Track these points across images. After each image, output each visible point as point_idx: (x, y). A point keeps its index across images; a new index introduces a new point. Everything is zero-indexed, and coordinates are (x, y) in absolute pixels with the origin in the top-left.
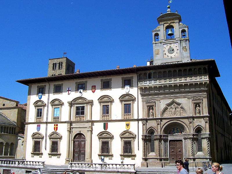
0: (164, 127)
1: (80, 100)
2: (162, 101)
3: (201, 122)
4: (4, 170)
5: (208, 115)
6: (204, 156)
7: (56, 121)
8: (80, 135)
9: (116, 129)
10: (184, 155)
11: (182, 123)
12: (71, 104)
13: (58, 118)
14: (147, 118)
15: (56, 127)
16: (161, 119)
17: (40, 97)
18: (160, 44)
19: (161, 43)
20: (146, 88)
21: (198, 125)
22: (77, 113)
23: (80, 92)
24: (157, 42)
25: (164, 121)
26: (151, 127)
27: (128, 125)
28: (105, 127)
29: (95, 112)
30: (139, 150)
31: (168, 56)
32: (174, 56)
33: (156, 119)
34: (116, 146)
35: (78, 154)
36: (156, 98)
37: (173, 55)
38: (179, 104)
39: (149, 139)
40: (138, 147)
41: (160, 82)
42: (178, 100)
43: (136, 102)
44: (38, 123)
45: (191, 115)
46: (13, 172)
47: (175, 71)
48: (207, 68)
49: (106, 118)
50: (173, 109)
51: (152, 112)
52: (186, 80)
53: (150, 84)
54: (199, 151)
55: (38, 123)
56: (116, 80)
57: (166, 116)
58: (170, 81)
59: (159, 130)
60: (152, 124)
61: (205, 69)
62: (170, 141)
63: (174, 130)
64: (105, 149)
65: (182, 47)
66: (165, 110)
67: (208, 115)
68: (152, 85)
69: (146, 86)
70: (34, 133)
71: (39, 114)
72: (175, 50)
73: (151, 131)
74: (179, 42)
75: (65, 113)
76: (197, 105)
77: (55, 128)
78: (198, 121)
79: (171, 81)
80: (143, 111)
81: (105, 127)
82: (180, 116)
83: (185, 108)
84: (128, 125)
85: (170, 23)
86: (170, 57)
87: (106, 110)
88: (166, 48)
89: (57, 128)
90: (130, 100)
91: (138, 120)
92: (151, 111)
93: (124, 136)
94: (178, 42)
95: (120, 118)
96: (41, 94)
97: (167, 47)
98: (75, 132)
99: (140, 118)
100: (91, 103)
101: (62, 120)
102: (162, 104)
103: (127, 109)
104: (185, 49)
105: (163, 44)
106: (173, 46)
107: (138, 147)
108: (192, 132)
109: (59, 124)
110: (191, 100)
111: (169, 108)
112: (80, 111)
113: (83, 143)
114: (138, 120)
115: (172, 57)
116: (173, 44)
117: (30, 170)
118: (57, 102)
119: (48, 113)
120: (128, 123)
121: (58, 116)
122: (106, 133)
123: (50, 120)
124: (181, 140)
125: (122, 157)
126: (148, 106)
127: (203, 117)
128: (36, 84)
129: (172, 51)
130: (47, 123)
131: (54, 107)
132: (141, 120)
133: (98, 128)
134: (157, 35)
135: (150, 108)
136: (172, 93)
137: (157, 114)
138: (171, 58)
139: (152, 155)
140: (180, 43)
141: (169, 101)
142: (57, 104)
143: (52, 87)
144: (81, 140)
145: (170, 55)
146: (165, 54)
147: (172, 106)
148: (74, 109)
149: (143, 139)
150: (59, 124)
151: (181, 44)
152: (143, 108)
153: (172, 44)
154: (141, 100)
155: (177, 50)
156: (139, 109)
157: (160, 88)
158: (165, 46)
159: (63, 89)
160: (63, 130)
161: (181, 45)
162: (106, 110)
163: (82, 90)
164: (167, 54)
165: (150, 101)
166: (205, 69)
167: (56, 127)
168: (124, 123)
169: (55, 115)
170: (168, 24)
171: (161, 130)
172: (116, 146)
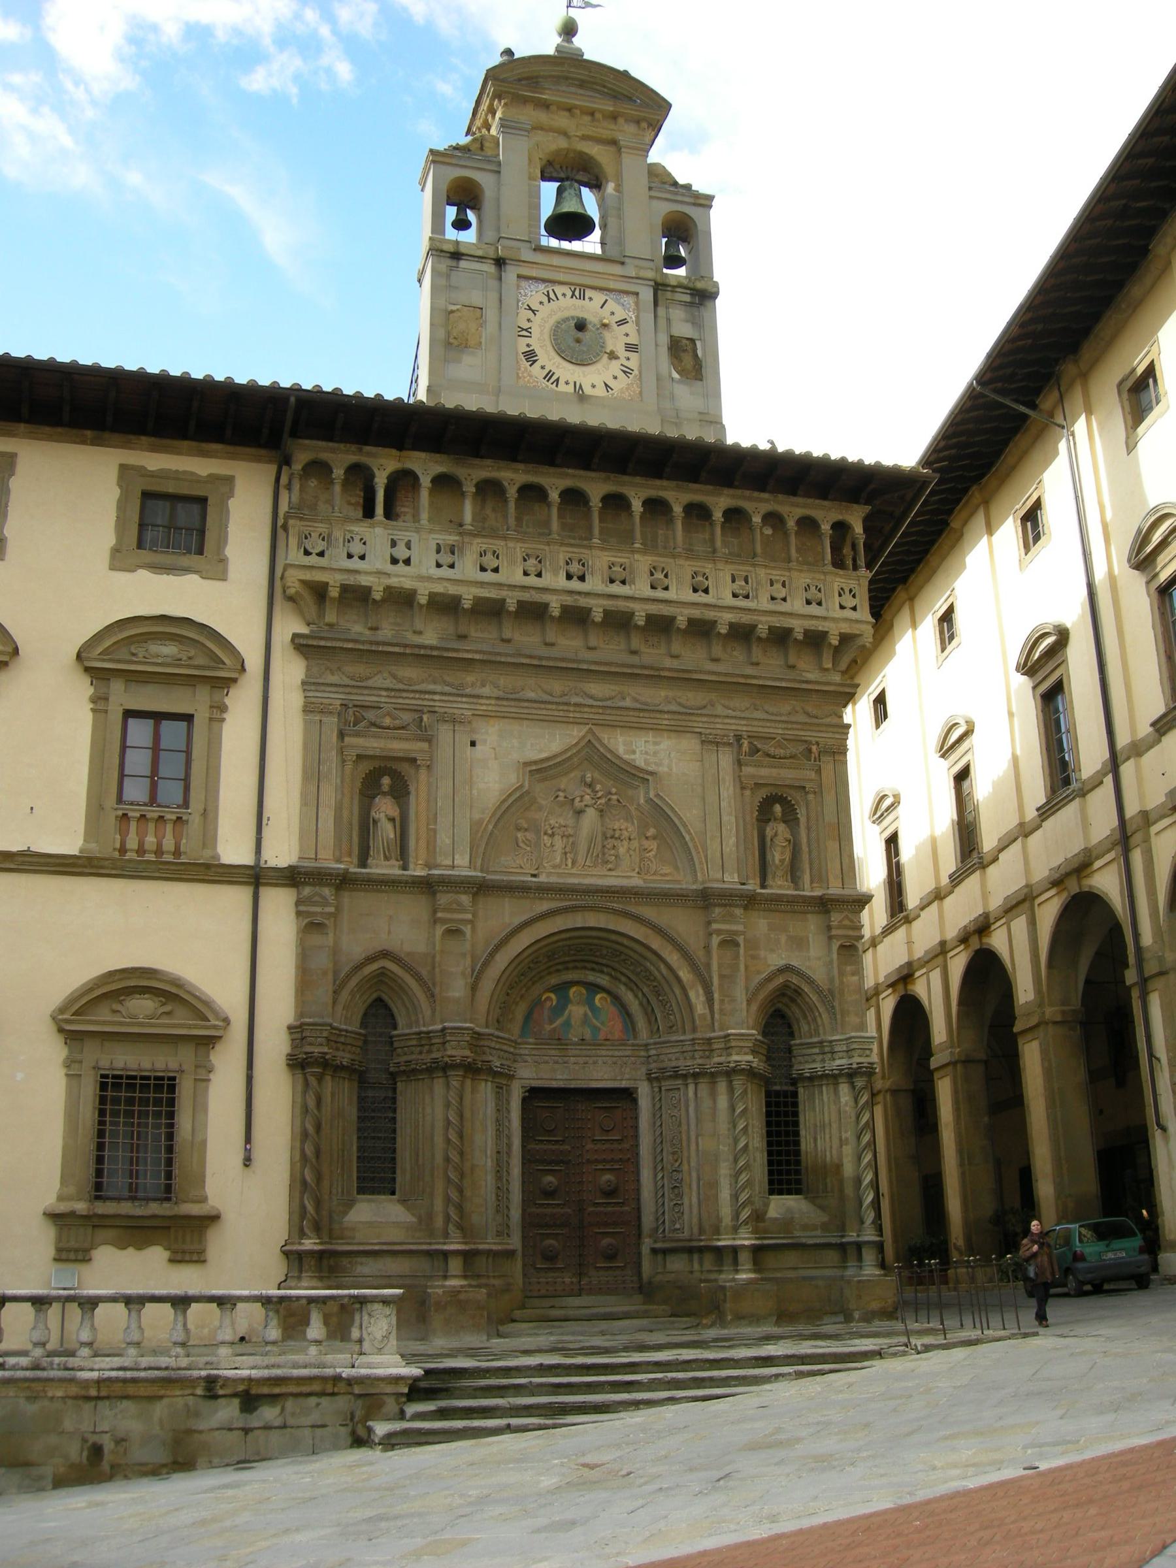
0: (502, 960)
2: (490, 734)
3: (799, 943)
6: (825, 1227)
10: (648, 1221)
11: (656, 943)
14: (352, 870)
16: (481, 889)
18: (490, 268)
19: (500, 262)
20: (356, 597)
21: (787, 969)
25: (503, 914)
26: (385, 954)
30: (248, 1161)
31: (549, 376)
32: (600, 392)
33: (428, 886)
36: (437, 702)
37: (594, 378)
39: (364, 1066)
40: (246, 1151)
41: (483, 569)
42: (638, 748)
43: (241, 708)
45: (731, 880)
47: (616, 503)
48: (858, 529)
50: (579, 812)
51: (392, 820)
52: (706, 591)
53: (401, 567)
54: (780, 1193)
57: (513, 866)
58: (569, 577)
59: (457, 989)
60: (398, 927)
61: (841, 528)
62: (534, 1095)
63: (561, 989)
65: (664, 340)
66: (515, 808)
68: (421, 578)
69: (364, 581)
72: (616, 340)
74: (647, 294)
78: (783, 939)
79: (582, 578)
80: (311, 800)
82: (636, 882)
83: (689, 814)
85: (585, 138)
86: (570, 389)
88: (543, 311)
90: (191, 681)
92: (385, 808)
93: (103, 1019)
94: (637, 294)
95: (70, 843)
99: (282, 852)
104: (688, 360)
105: (519, 277)
107: (246, 1151)
110: (726, 759)
114: (256, 877)
115: (588, 390)
116: (599, 298)
124: (627, 1095)
126: (360, 757)
129: (578, 340)
132: (292, 877)
137: (444, 839)
138: (580, 396)
139: (376, 1218)
140: (656, 304)
141: (550, 742)
145: (567, 372)
146: (531, 356)
149: (298, 1063)
151: (661, 311)
152: (313, 775)
153: (589, 293)
154: (296, 700)
155: (631, 348)
156: (263, 773)
158: (534, 294)
161: (662, 322)
164: (548, 358)
165: (387, 721)
166: (841, 528)
170: (563, 143)
171: (474, 988)
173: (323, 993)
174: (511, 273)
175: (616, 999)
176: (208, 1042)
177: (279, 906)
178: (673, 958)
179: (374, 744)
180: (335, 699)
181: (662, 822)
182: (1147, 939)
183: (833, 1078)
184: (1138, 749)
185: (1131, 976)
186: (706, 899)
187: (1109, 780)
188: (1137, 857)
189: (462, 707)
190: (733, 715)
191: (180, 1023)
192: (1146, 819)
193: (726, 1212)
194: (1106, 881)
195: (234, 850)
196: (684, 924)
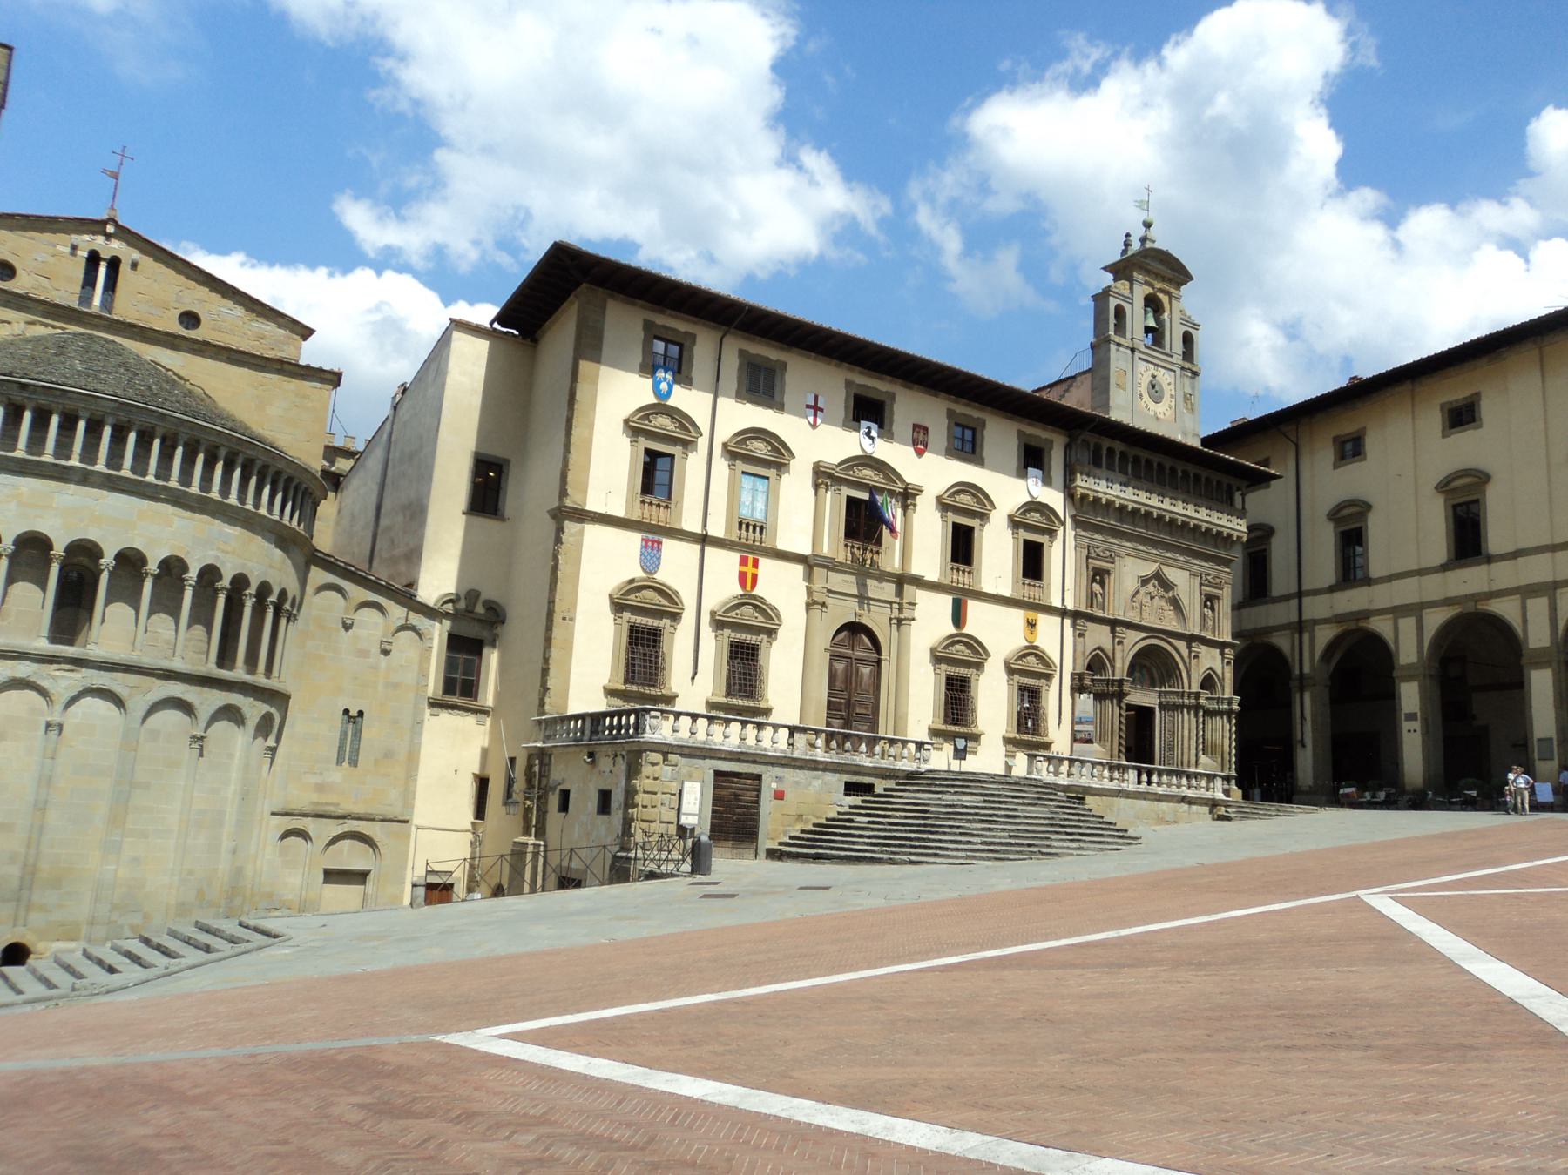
1: (868, 472)
4: (718, 774)
5: (1227, 637)
7: (751, 541)
8: (854, 629)
9: (1000, 631)
12: (823, 476)
13: (762, 528)
15: (749, 569)
16: (1129, 625)
17: (664, 386)
19: (1133, 350)
22: (851, 533)
23: (868, 434)
24: (1122, 341)
27: (1032, 625)
28: (958, 617)
29: (922, 542)
33: (1113, 624)
34: (993, 701)
35: (842, 717)
37: (1162, 409)
38: (1166, 585)
44: (655, 533)
46: (774, 785)
49: (963, 580)
55: (655, 533)
56: (1001, 435)
57: (1132, 617)
64: (957, 701)
67: (1227, 637)
70: (632, 581)
71: (655, 476)
72: (1168, 391)
73: (1097, 663)
74: (1178, 371)
75: (801, 516)
76: (1209, 601)
77: (742, 577)
81: (958, 617)
84: (1032, 625)
85: (1161, 290)
87: (962, 547)
89: (755, 577)
91: (1063, 613)
96: (669, 377)
97: (1144, 372)
98: (847, 611)
99: (1070, 606)
100: (908, 496)
101: (781, 545)
102: (1131, 569)
103: (1032, 563)
106: (1164, 377)
108: (1195, 688)
109: (763, 561)
111: (1143, 590)
112: (864, 523)
113: (866, 671)
114: (1063, 613)
117: (867, 780)
118: (759, 448)
119: (705, 488)
120: (1031, 615)
121: (759, 515)
122: (966, 644)
123: (717, 529)
125: (1011, 747)
127: (1222, 646)
128: (634, 304)
130: (704, 540)
131: (741, 466)
132: (1076, 615)
133: (931, 618)
134: (1120, 312)
135: (1099, 576)
136: (1155, 544)
141: (1149, 569)
142: (760, 456)
143: (731, 363)
144: (859, 653)
145: (1152, 405)
147: (1150, 587)
148: (834, 504)
150: (763, 561)
157: (1122, 512)
158: (1141, 366)
159: (787, 389)
160: (782, 587)
162: (962, 547)
163: (874, 426)
164: (1146, 397)
167: (749, 569)
168: (1017, 616)
169: (745, 512)
172: (993, 701)
173: (1080, 661)
174: (1137, 355)
175: (1149, 671)
176: (1048, 677)
177: (1067, 622)
178: (1178, 659)
179: (1098, 563)
180: (1085, 542)
181: (1176, 604)
182: (1307, 669)
183: (1220, 713)
184: (1316, 592)
185: (1294, 684)
186: (1190, 639)
187: (1294, 602)
188: (1306, 637)
189: (1122, 551)
190: (1199, 565)
191: (1041, 669)
192: (1315, 622)
193: (1193, 759)
194: (1283, 642)
195: (1057, 603)
196: (1182, 645)
